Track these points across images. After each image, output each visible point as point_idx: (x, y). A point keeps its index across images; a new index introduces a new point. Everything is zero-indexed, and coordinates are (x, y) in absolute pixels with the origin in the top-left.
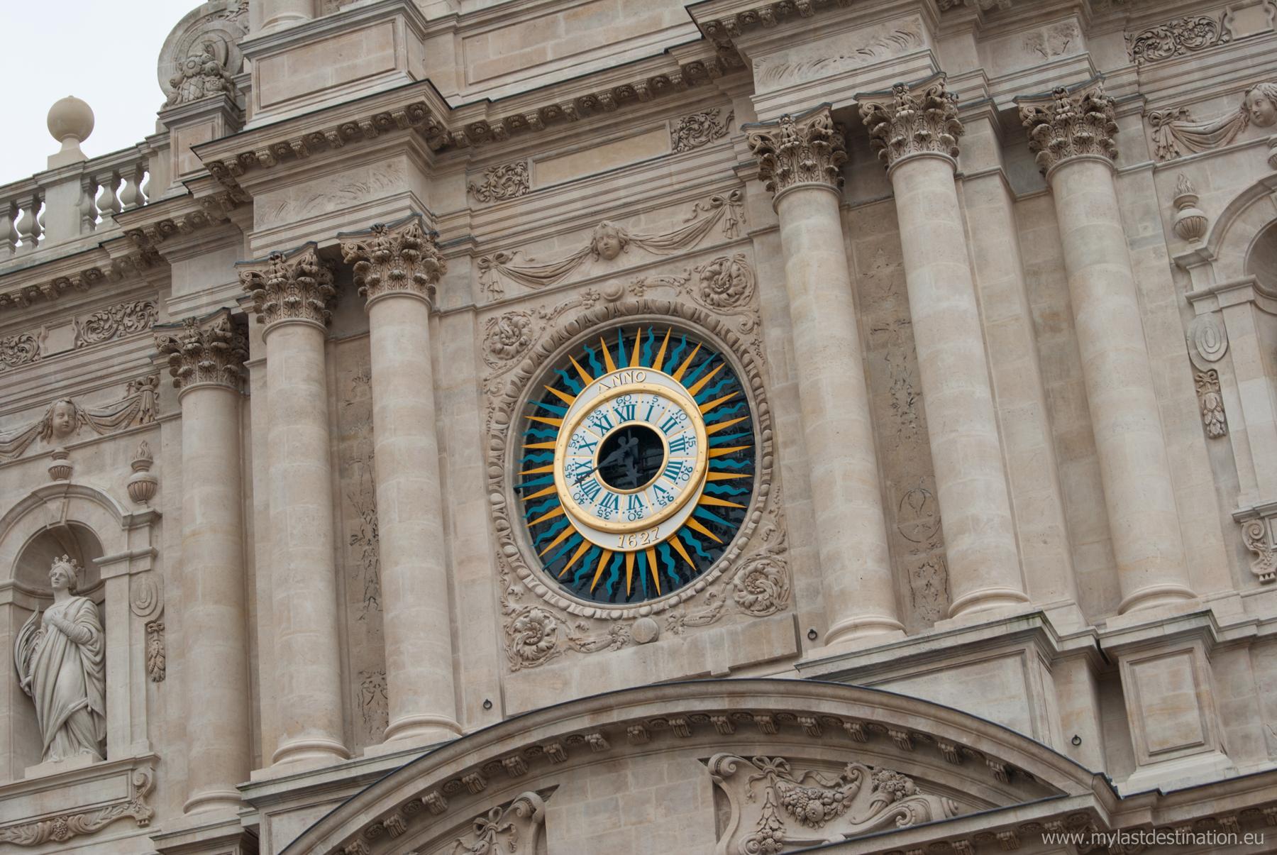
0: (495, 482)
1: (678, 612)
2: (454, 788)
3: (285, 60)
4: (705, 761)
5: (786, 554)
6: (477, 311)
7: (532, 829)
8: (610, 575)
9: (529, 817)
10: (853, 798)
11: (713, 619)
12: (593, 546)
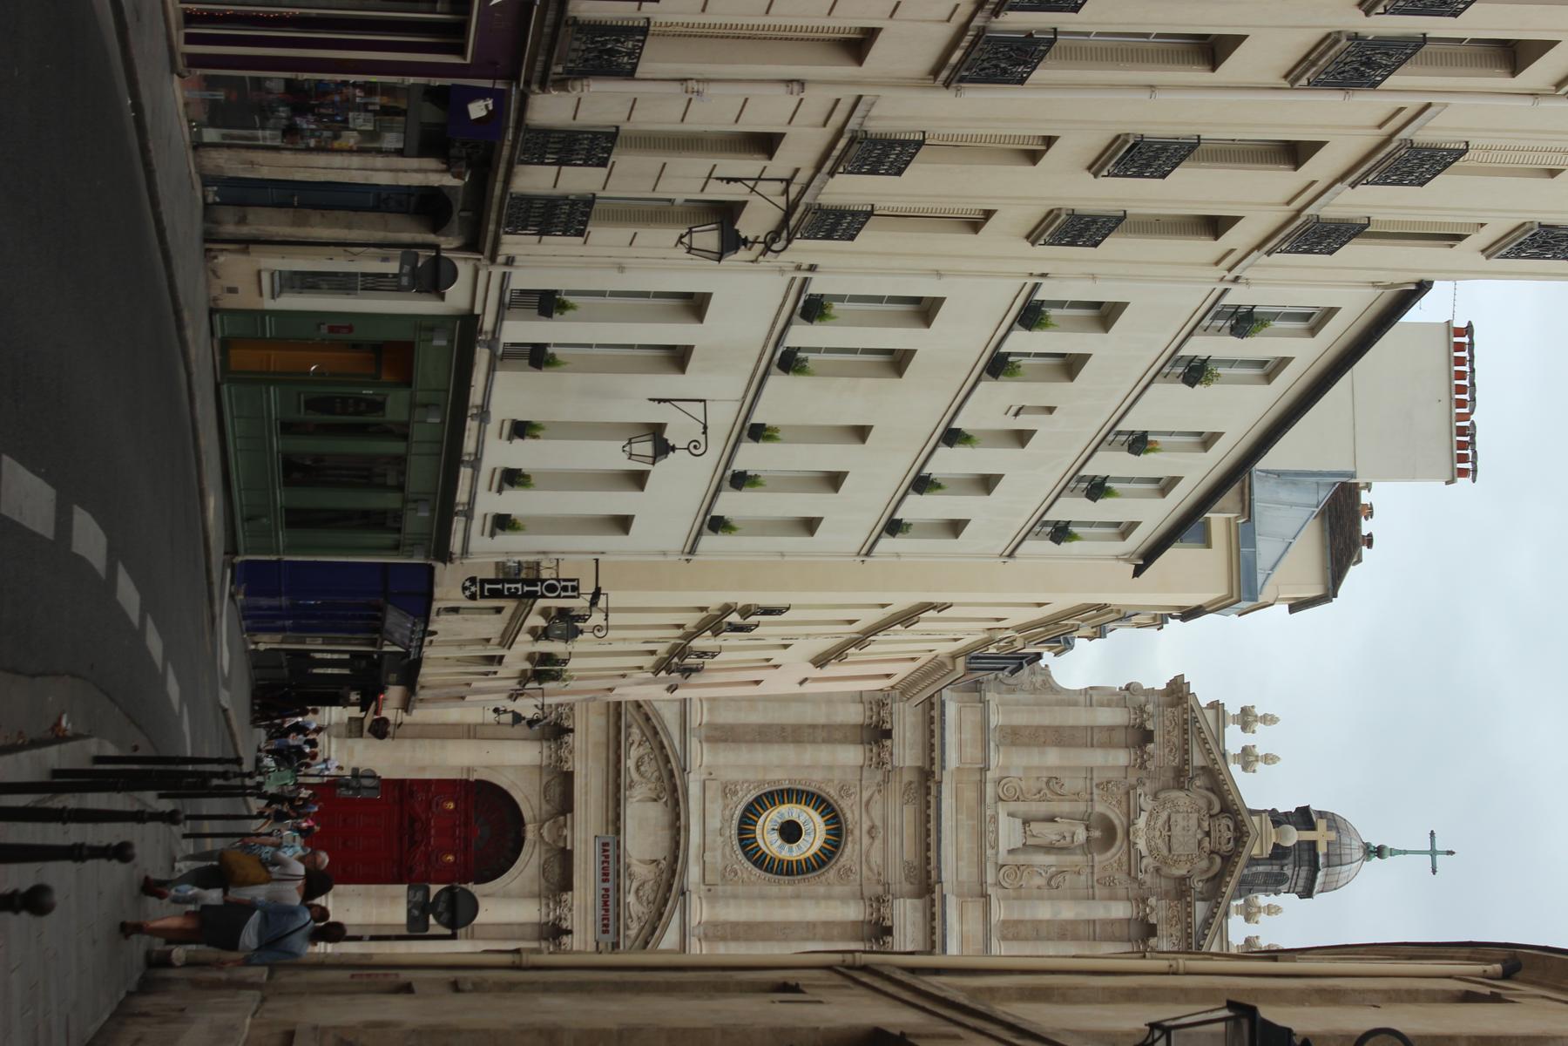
3: (978, 718)
11: (724, 855)
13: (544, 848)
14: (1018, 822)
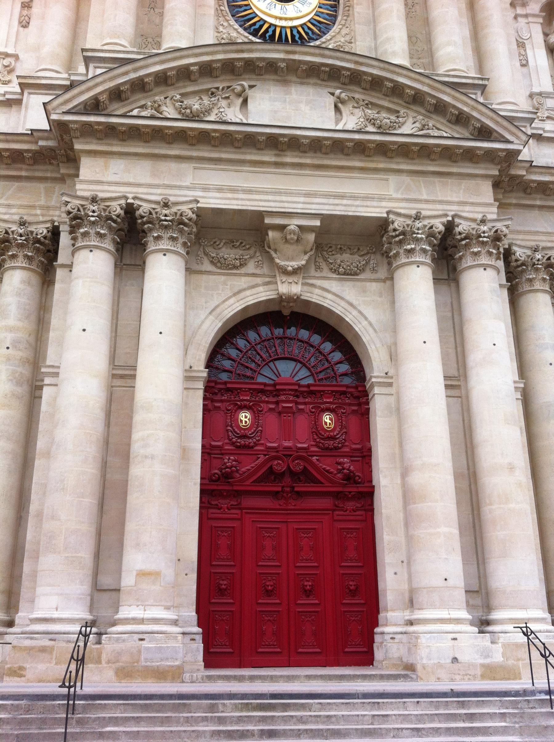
2: (207, 70)
4: (333, 94)
5: (352, 45)
7: (241, 100)
8: (268, 32)
9: (239, 95)
10: (402, 125)
13: (313, 272)
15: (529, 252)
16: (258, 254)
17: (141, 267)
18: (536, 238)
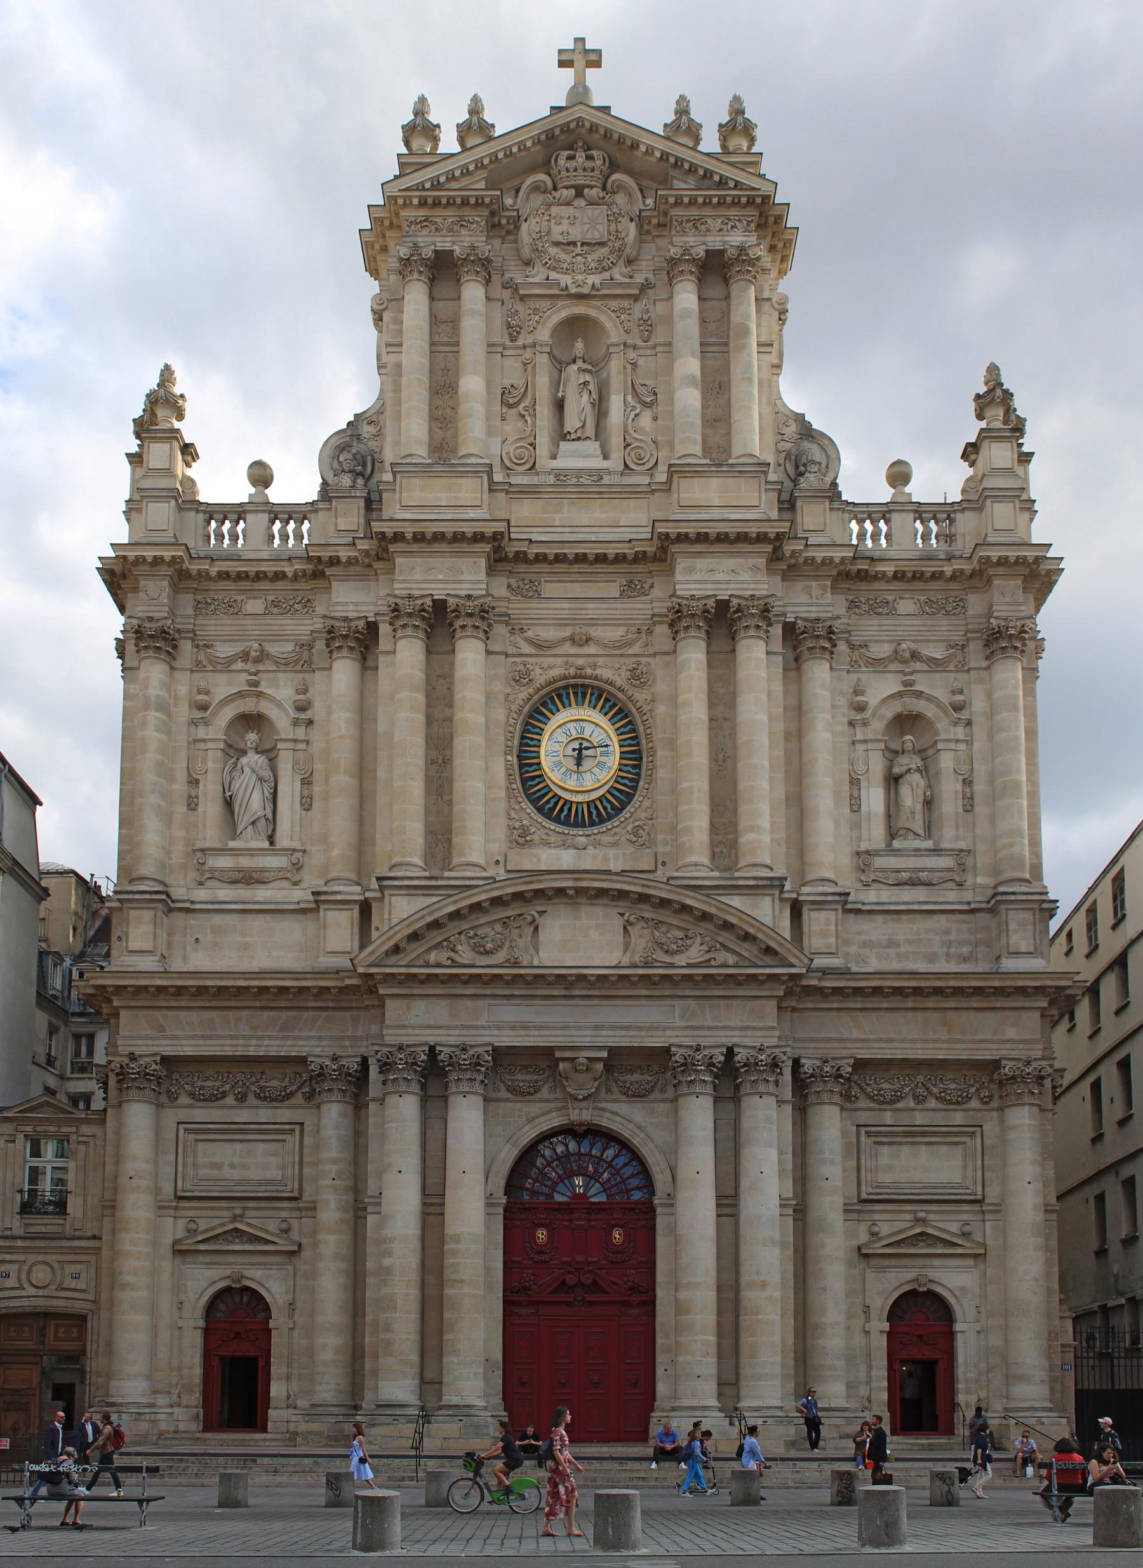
0: (508, 750)
1: (598, 837)
6: (507, 655)
11: (614, 845)
12: (556, 794)
14: (563, 445)
15: (818, 1063)
16: (551, 1079)
17: (445, 1099)
18: (829, 1045)
